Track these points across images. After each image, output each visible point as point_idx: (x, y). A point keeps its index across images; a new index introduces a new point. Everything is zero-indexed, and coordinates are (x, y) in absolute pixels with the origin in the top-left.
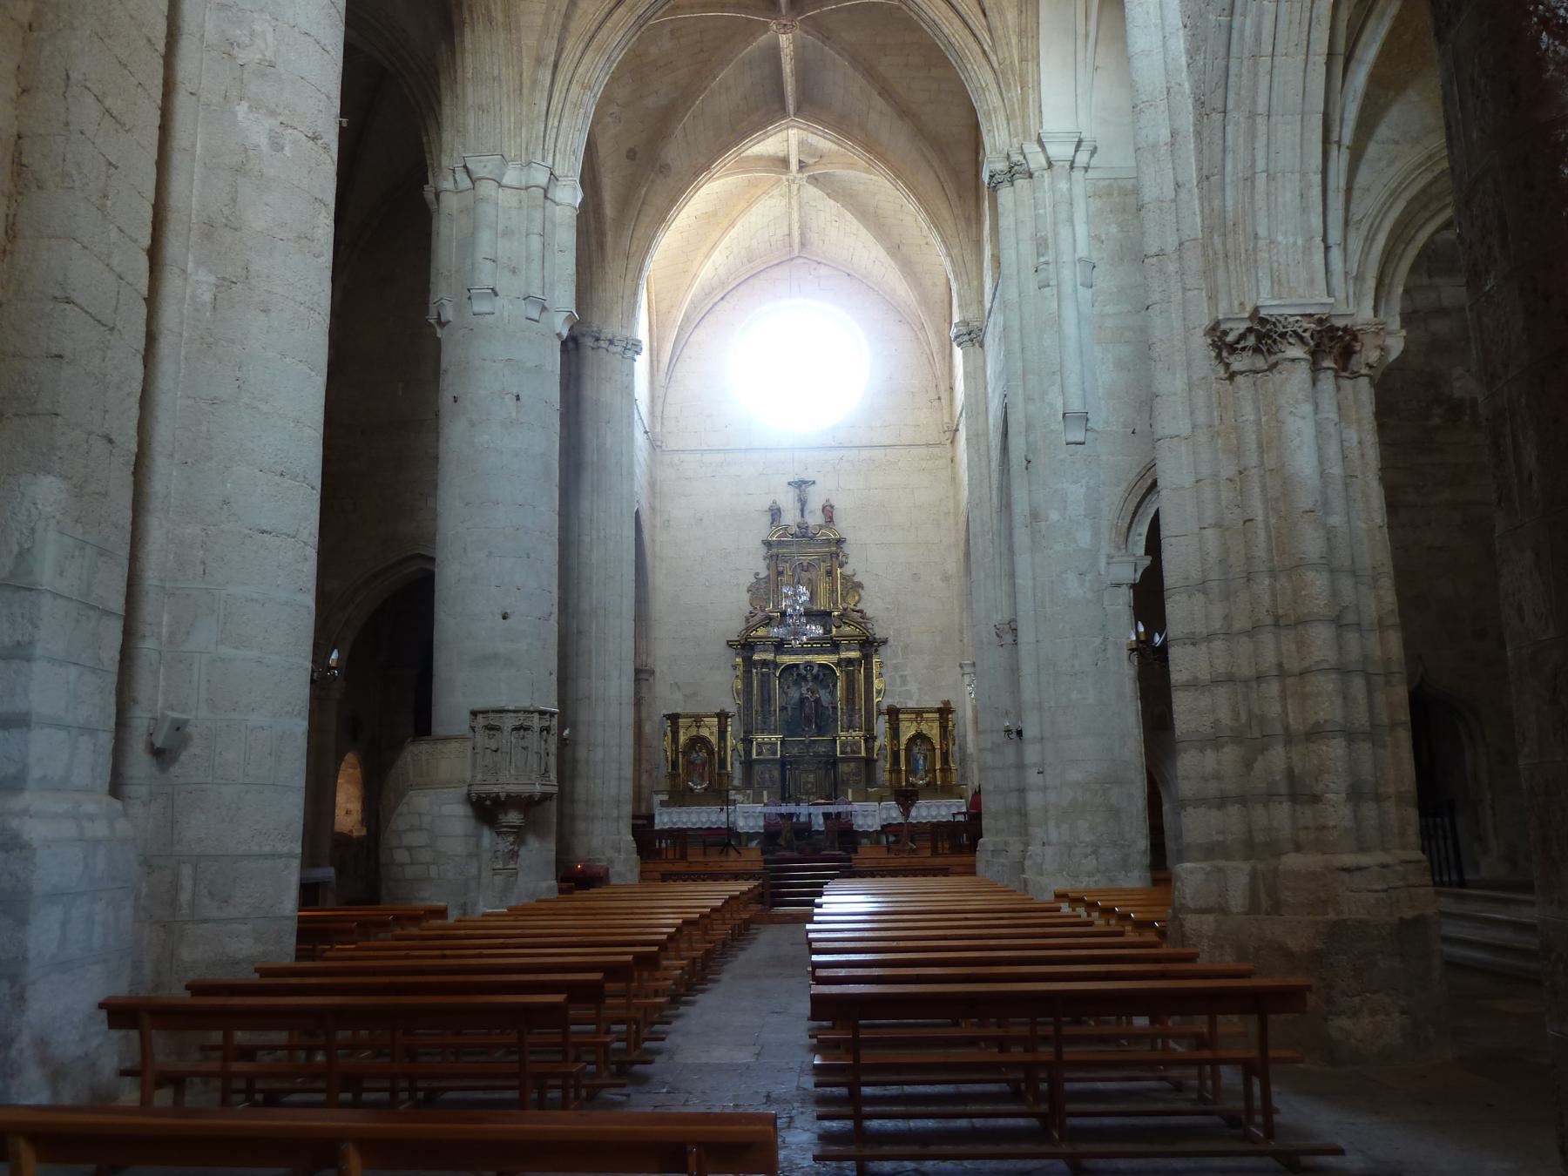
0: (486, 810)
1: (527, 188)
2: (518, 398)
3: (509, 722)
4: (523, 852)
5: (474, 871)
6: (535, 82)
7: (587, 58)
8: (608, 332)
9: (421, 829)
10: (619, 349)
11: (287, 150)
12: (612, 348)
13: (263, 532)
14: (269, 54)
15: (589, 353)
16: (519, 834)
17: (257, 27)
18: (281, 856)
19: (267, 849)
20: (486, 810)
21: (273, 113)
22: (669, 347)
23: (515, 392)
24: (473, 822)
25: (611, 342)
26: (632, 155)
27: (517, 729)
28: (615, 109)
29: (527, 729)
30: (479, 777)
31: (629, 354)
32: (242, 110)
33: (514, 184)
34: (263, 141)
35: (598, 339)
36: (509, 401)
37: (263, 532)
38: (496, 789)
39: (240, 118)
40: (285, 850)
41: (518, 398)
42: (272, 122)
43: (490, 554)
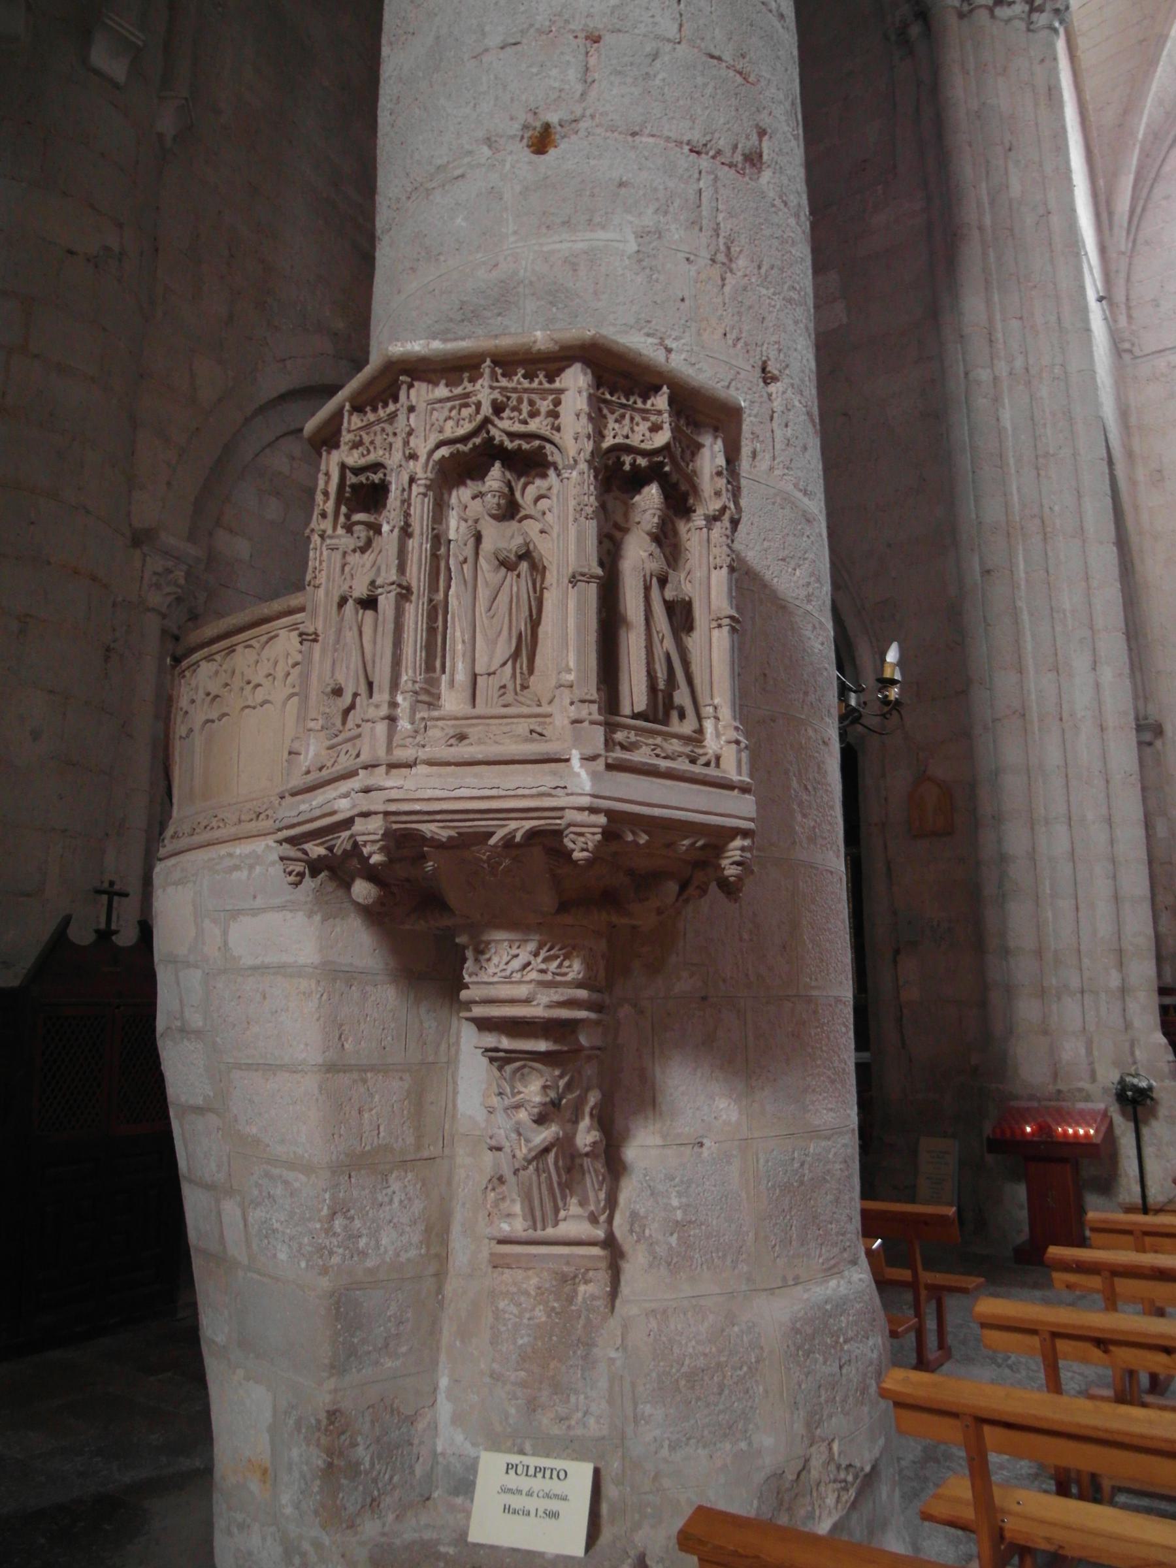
4: (643, 1148)
16: (596, 1078)
22: (1126, 183)
27: (463, 466)
38: (340, 801)
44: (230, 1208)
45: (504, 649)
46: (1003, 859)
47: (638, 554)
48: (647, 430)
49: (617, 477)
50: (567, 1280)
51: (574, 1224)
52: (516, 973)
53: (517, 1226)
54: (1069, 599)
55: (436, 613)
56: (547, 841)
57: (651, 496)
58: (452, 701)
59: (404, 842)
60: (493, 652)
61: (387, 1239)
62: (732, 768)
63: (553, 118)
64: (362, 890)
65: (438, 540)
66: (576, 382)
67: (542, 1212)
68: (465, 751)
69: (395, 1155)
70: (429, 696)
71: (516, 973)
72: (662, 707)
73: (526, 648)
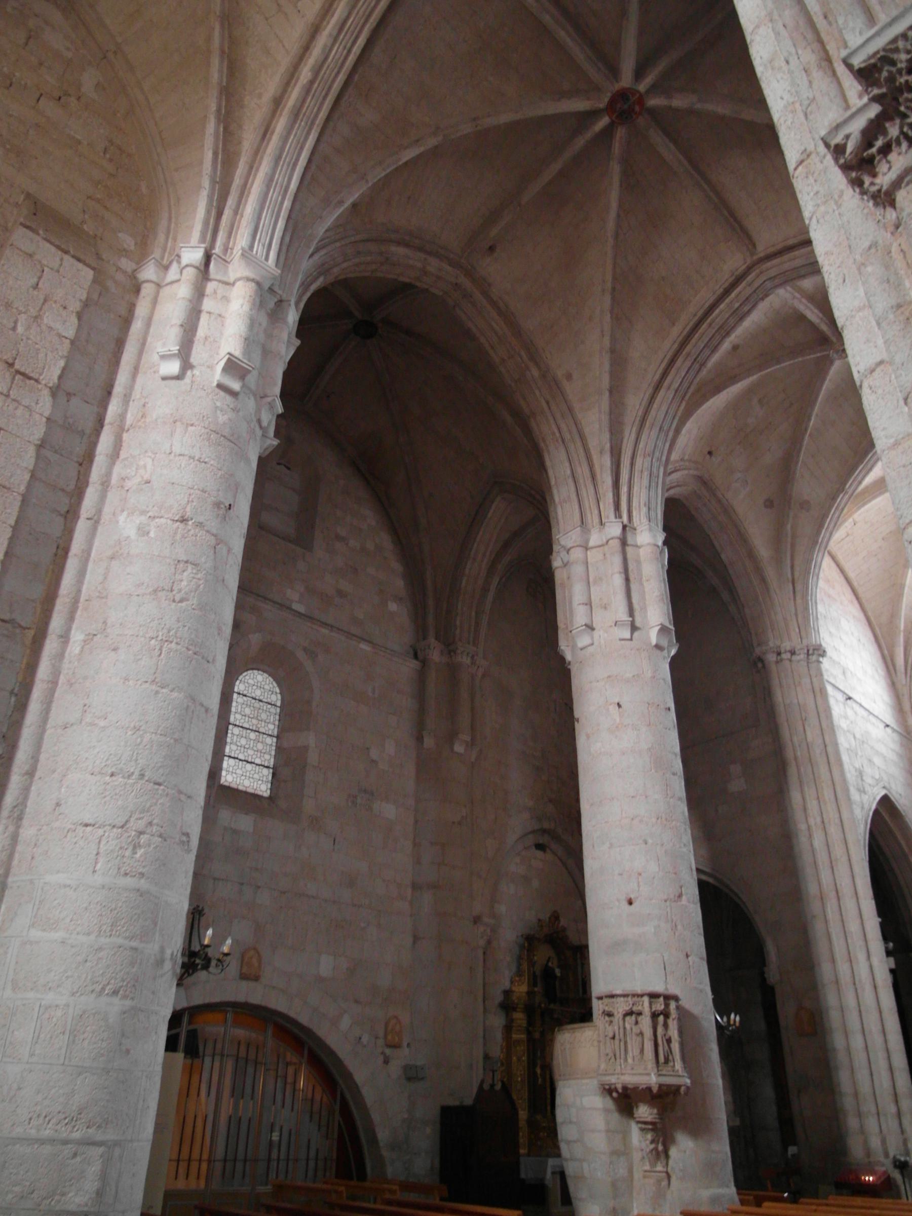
0: (625, 1100)
1: (607, 542)
2: (619, 705)
3: (621, 1006)
4: (673, 1152)
5: (622, 1172)
6: (601, 467)
7: (644, 437)
8: (787, 645)
9: (571, 1122)
10: (802, 656)
11: (152, 534)
12: (795, 658)
13: (87, 825)
14: (146, 477)
15: (773, 667)
17: (142, 463)
18: (65, 1142)
19: (47, 1133)
20: (625, 1100)
21: (143, 513)
23: (616, 701)
24: (616, 1116)
25: (793, 653)
26: (769, 504)
28: (739, 475)
29: (640, 1014)
30: (603, 1066)
31: (814, 658)
32: (122, 518)
33: (599, 543)
34: (132, 533)
35: (779, 654)
36: (613, 709)
37: (87, 825)
38: (613, 1080)
39: (121, 523)
40: (76, 1135)
41: (619, 705)
42: (144, 519)
43: (611, 846)
44: (585, 1165)
45: (638, 1051)
46: (834, 1050)
47: (660, 1030)
48: (659, 1006)
49: (654, 1016)
50: (659, 1181)
51: (659, 1167)
52: (644, 1112)
53: (647, 1167)
54: (853, 927)
55: (626, 1043)
56: (649, 1089)
57: (661, 1019)
58: (630, 1061)
59: (625, 1088)
60: (637, 1052)
61: (621, 1170)
62: (680, 1073)
63: (632, 896)
64: (615, 1095)
65: (625, 1028)
66: (646, 999)
67: (653, 1165)
68: (634, 1072)
69: (621, 1152)
70: (626, 1060)
71: (644, 1112)
72: (667, 1061)
73: (642, 1051)
